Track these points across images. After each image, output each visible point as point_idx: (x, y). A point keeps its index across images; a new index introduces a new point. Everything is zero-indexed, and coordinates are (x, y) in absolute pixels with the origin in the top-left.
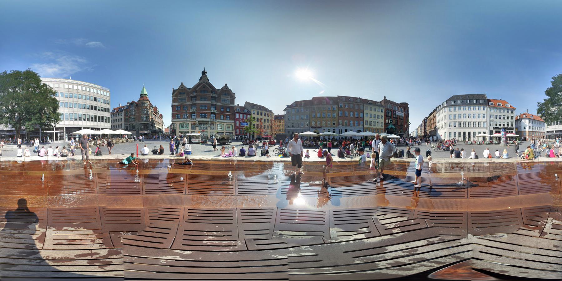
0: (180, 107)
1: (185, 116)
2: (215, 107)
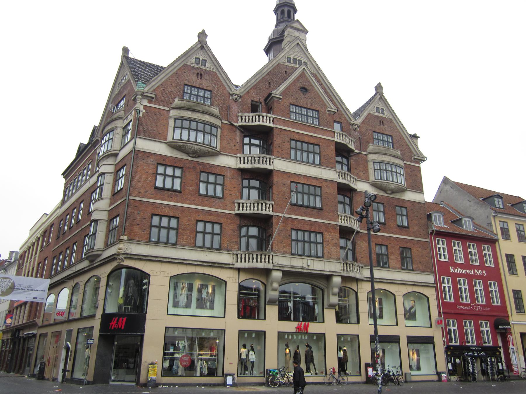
1: (204, 233)
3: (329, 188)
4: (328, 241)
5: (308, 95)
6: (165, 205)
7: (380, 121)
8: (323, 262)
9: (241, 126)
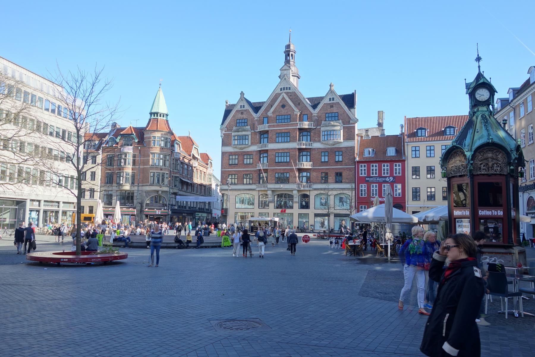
0: (237, 157)
2: (309, 154)
5: (285, 108)
9: (259, 131)
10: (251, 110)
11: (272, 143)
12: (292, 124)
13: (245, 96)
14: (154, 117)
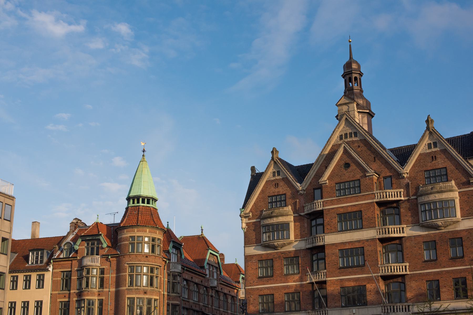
3: (370, 246)
4: (370, 291)
5: (350, 169)
6: (265, 288)
7: (432, 157)
8: (367, 309)
10: (291, 178)
11: (331, 233)
12: (363, 195)
13: (280, 156)
14: (133, 205)
